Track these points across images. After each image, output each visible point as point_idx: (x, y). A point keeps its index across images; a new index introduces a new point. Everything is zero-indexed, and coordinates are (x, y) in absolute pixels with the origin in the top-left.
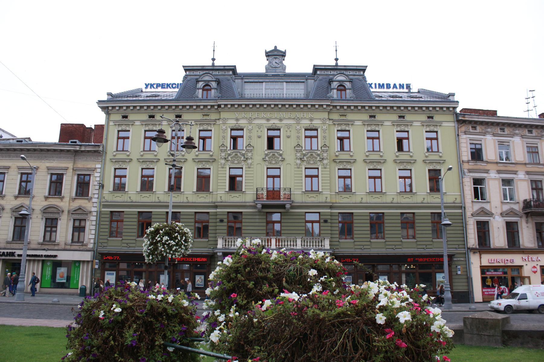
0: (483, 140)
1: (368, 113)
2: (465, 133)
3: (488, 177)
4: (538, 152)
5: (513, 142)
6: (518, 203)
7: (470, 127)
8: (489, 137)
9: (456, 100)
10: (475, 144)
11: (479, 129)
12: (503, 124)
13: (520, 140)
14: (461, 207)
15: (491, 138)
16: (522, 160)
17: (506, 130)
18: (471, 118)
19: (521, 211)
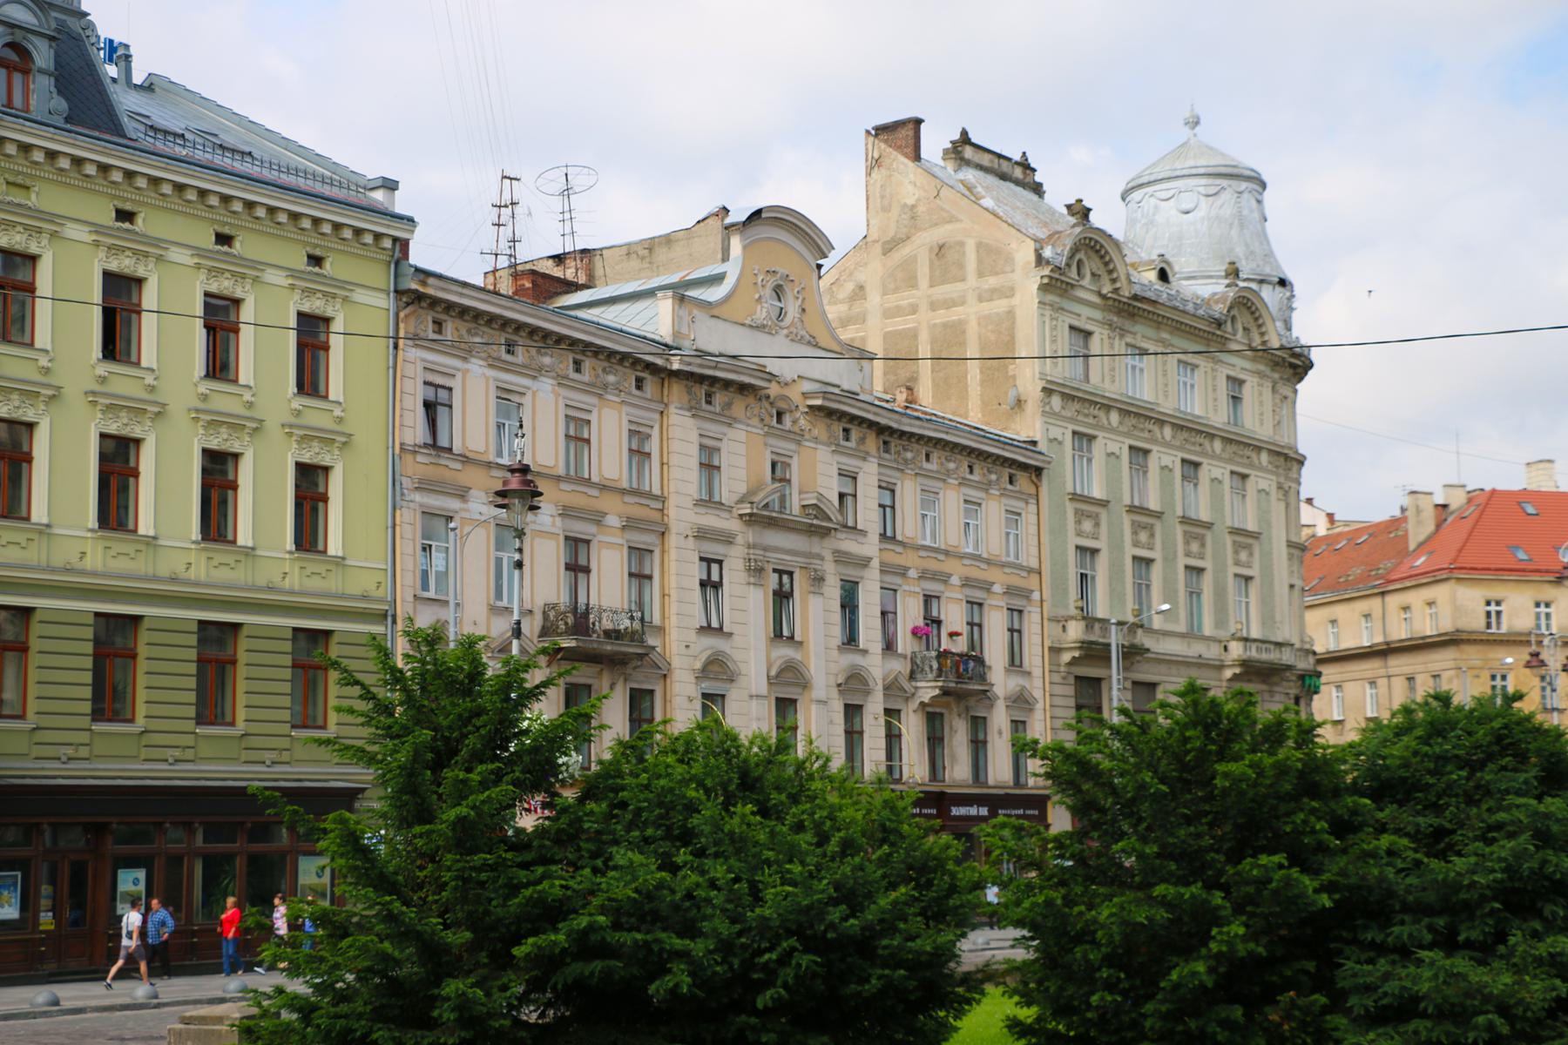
0: (459, 375)
1: (114, 197)
2: (415, 338)
3: (464, 515)
4: (588, 441)
5: (534, 394)
6: (531, 611)
7: (430, 319)
8: (476, 367)
9: (399, 209)
10: (437, 386)
11: (451, 329)
12: (449, 307)
13: (553, 391)
14: (382, 617)
15: (480, 371)
16: (552, 463)
17: (519, 350)
18: (443, 289)
19: (535, 641)
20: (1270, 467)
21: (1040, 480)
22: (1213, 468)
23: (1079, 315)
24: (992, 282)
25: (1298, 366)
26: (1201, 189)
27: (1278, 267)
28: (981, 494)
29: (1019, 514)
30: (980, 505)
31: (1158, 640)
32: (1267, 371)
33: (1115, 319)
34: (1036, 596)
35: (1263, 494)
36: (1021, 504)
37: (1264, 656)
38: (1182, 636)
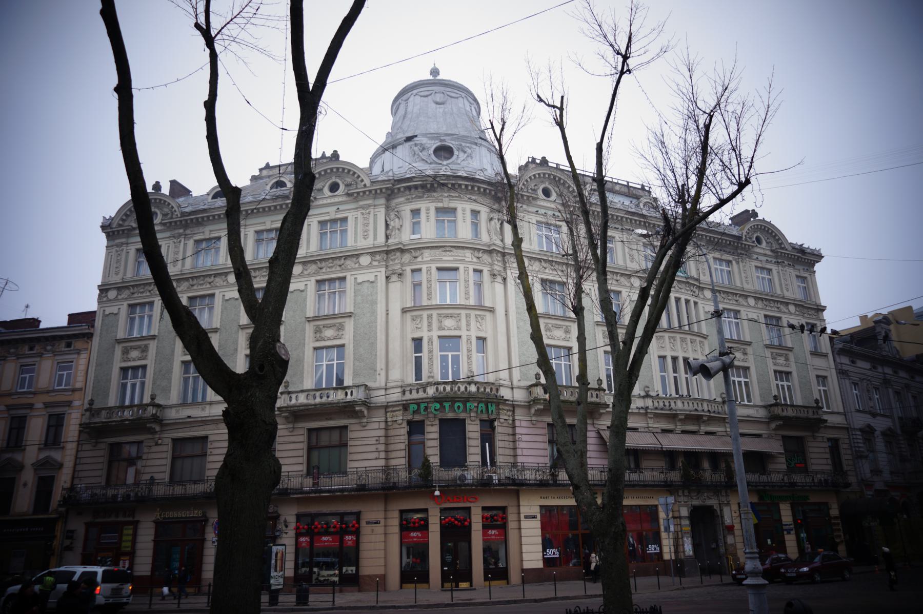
20: (376, 263)
29: (72, 362)
33: (181, 231)
34: (77, 403)
35: (366, 284)
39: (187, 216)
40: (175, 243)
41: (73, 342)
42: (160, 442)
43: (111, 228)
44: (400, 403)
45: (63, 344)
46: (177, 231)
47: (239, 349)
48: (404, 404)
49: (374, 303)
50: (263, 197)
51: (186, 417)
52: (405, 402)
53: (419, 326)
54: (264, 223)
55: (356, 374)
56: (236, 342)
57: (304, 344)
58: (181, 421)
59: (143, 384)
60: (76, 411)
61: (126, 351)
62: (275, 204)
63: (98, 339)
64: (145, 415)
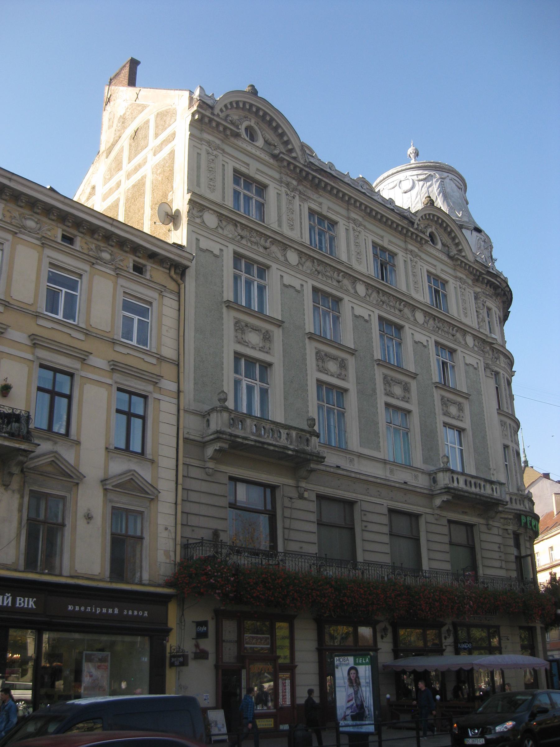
20: (476, 349)
21: (184, 282)
22: (416, 335)
23: (248, 165)
24: (163, 136)
25: (498, 287)
26: (415, 178)
27: (474, 222)
28: (87, 267)
29: (150, 304)
30: (80, 276)
31: (351, 461)
32: (470, 282)
33: (295, 183)
35: (471, 369)
36: (156, 295)
37: (473, 489)
38: (385, 462)
39: (313, 170)
40: (287, 195)
41: (149, 268)
42: (306, 495)
43: (213, 114)
44: (513, 511)
45: (129, 261)
46: (289, 179)
47: (378, 391)
48: (516, 514)
49: (479, 393)
50: (393, 208)
51: (335, 466)
52: (518, 512)
53: (506, 434)
54: (382, 237)
55: (477, 469)
56: (373, 380)
57: (435, 414)
58: (332, 470)
59: (264, 393)
60: (167, 399)
61: (240, 327)
62: (400, 223)
63: (194, 284)
64: (309, 448)
